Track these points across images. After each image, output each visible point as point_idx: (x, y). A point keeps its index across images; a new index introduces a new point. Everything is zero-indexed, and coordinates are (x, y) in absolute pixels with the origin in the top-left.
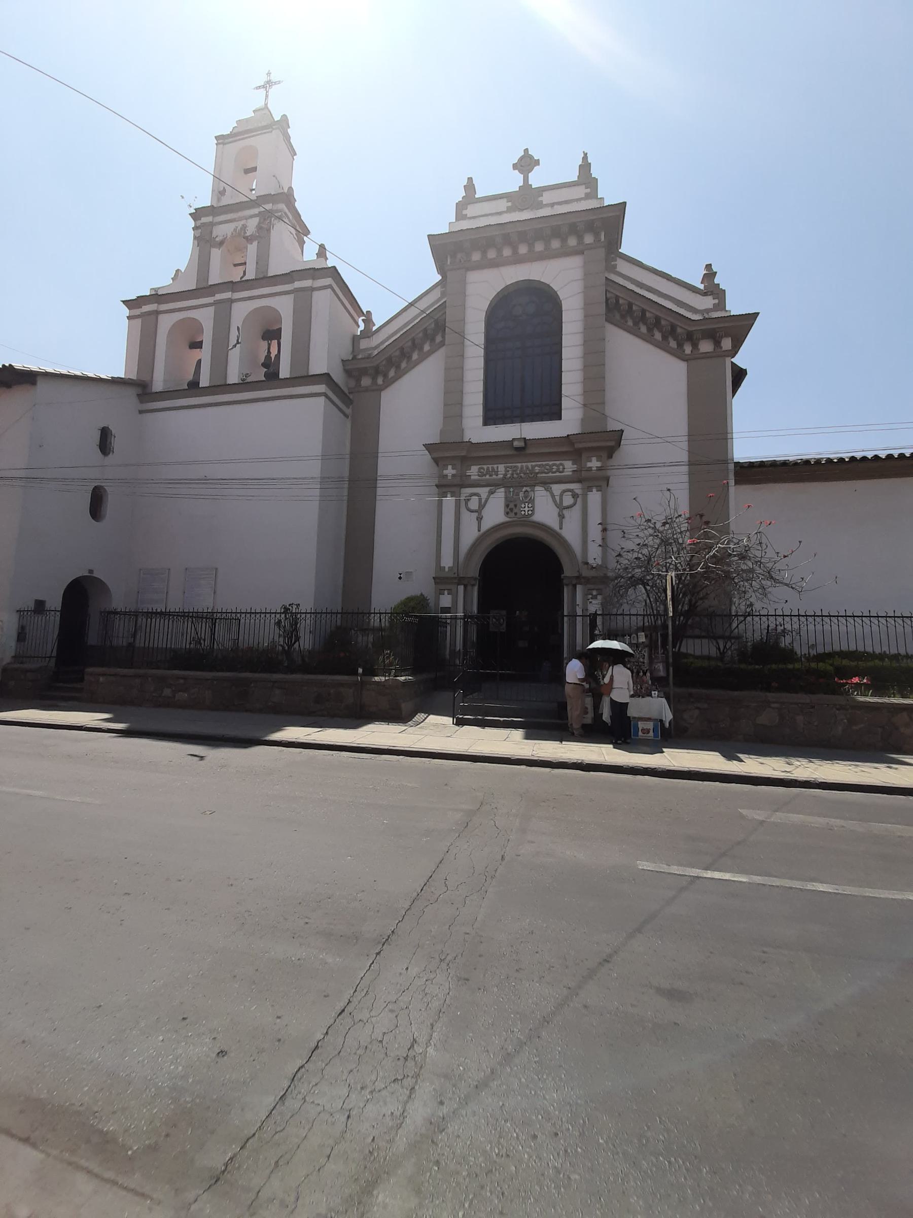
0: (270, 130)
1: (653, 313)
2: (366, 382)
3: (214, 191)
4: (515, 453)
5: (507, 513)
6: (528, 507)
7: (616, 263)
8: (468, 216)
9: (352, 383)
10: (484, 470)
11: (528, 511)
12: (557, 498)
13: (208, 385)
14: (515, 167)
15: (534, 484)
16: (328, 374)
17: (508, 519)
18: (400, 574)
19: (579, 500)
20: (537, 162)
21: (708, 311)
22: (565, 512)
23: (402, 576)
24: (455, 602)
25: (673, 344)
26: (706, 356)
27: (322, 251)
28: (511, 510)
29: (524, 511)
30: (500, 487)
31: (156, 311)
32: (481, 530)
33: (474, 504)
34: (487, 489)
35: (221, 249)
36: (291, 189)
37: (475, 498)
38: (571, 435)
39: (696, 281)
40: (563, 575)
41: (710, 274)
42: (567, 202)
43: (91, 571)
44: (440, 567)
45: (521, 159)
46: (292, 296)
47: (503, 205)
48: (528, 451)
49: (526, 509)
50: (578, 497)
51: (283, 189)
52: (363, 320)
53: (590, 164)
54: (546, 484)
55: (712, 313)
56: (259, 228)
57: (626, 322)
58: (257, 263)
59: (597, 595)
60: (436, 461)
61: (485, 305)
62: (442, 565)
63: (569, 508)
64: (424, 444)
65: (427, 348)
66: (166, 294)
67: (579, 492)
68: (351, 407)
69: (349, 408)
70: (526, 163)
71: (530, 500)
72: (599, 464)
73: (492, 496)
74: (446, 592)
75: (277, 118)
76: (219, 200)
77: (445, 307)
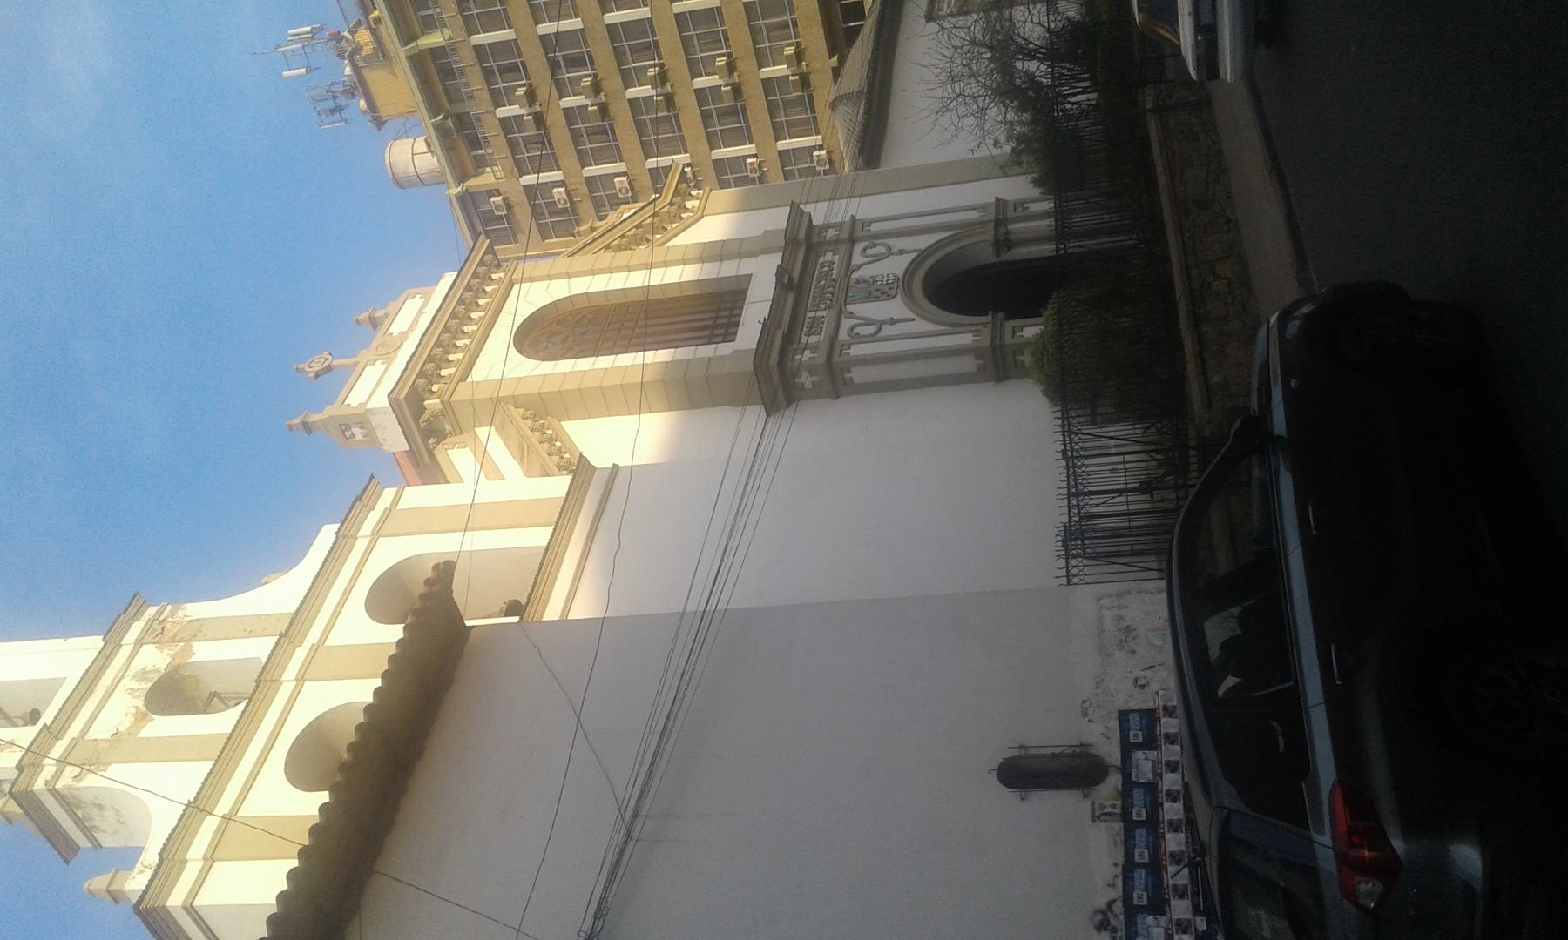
5: (888, 296)
8: (364, 401)
22: (895, 250)
28: (883, 293)
37: (856, 330)
54: (848, 268)
58: (251, 632)
62: (970, 341)
66: (204, 784)
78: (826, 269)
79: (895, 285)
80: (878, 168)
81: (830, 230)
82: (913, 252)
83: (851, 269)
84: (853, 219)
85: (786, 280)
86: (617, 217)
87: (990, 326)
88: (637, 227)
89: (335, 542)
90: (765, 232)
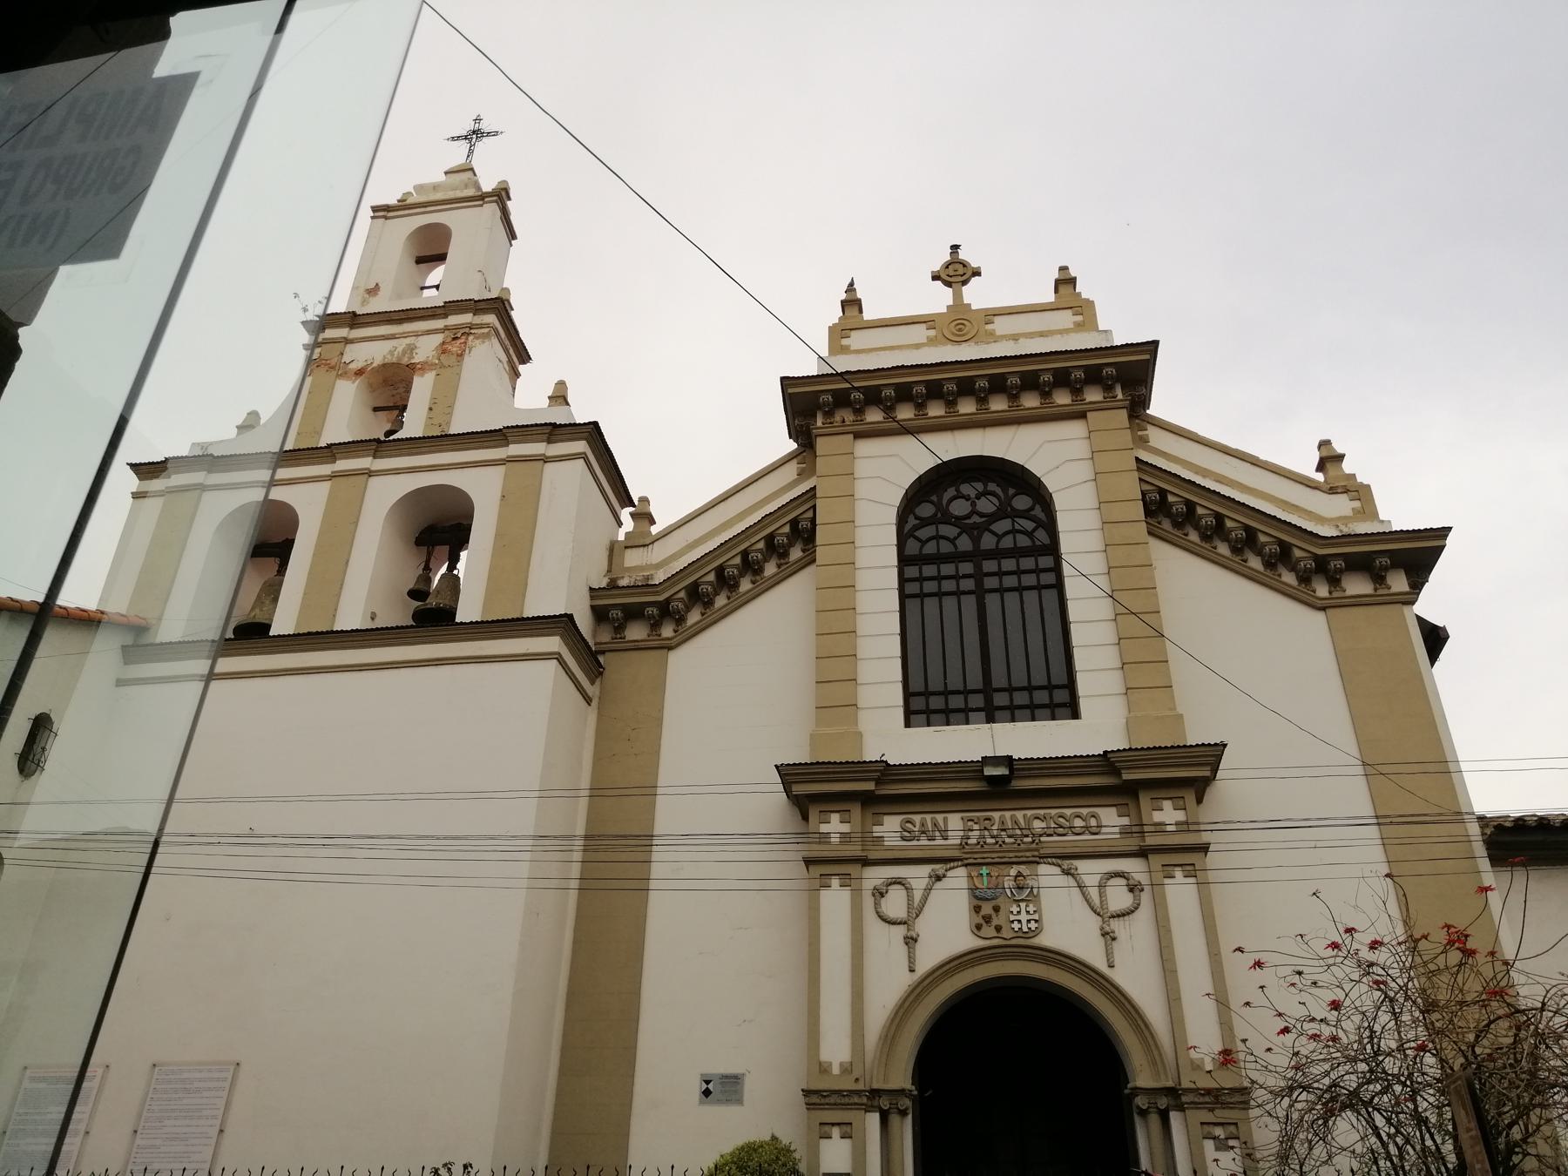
0: (481, 202)
1: (1242, 523)
3: (357, 288)
5: (979, 927)
6: (1028, 912)
7: (1145, 432)
8: (852, 348)
9: (606, 636)
10: (915, 826)
11: (1029, 921)
12: (1094, 893)
13: (289, 629)
14: (935, 277)
15: (1037, 859)
16: (570, 617)
17: (981, 943)
18: (707, 1082)
19: (1145, 897)
20: (977, 273)
21: (1345, 519)
22: (1115, 925)
23: (711, 1086)
24: (859, 1156)
25: (1289, 578)
27: (560, 397)
28: (988, 919)
29: (1019, 921)
30: (956, 864)
31: (201, 484)
32: (916, 969)
33: (895, 904)
34: (925, 870)
35: (357, 382)
38: (1113, 751)
40: (1129, 1086)
41: (1329, 459)
42: (1042, 334)
44: (820, 1063)
45: (947, 266)
46: (501, 469)
47: (920, 333)
49: (1021, 916)
50: (1142, 890)
51: (490, 291)
52: (632, 515)
53: (1075, 278)
54: (1064, 859)
55: (1355, 524)
56: (443, 350)
57: (1186, 535)
58: (431, 409)
59: (1227, 1139)
60: (803, 805)
61: (896, 497)
62: (825, 1056)
63: (1124, 915)
64: (779, 763)
65: (770, 569)
67: (1143, 878)
68: (598, 682)
69: (593, 683)
70: (956, 272)
71: (1027, 896)
72: (1180, 816)
73: (938, 885)
74: (836, 1132)
75: (487, 186)
76: (364, 302)
77: (814, 496)
78: (1078, 823)
80: (1493, 865)
81: (1180, 816)
82: (1109, 954)
83: (1066, 864)
84: (1204, 849)
85: (989, 771)
86: (1331, 488)
87: (860, 1086)
88: (1247, 528)
89: (495, 431)
90: (1182, 715)
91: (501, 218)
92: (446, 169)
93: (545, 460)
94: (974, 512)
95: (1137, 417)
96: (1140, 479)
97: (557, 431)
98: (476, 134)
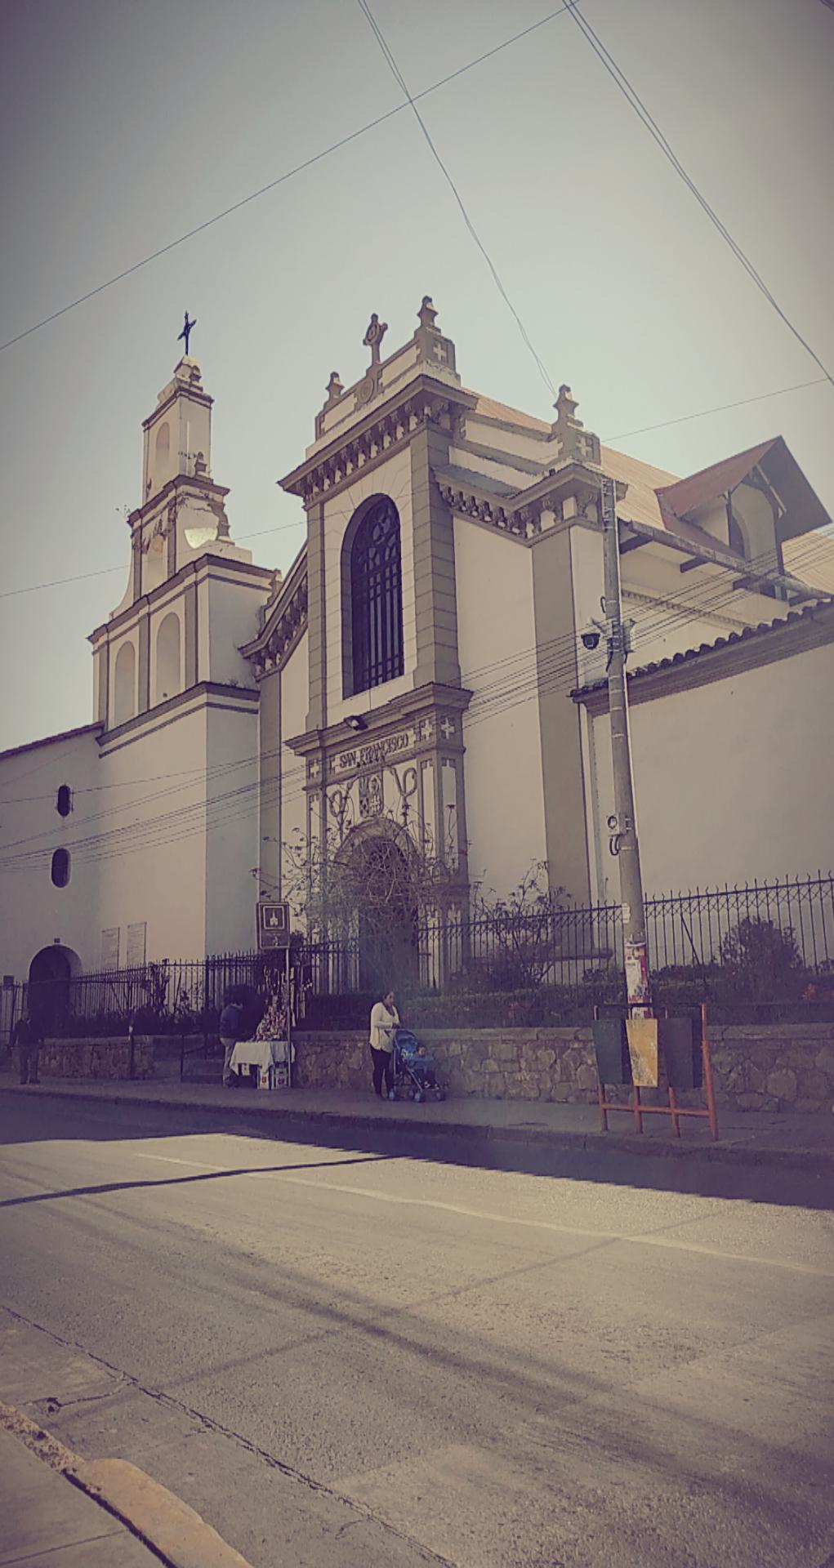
2: (269, 662)
4: (359, 732)
5: (361, 812)
9: (258, 668)
26: (552, 533)
28: (365, 806)
36: (201, 455)
39: (550, 417)
43: (57, 940)
47: (352, 400)
48: (370, 728)
49: (374, 802)
56: (169, 520)
69: (257, 700)
70: (375, 333)
76: (147, 495)
78: (400, 742)
79: (371, 813)
91: (190, 399)
92: (174, 368)
93: (196, 584)
94: (379, 538)
95: (459, 417)
96: (435, 484)
97: (197, 564)
98: (188, 327)
